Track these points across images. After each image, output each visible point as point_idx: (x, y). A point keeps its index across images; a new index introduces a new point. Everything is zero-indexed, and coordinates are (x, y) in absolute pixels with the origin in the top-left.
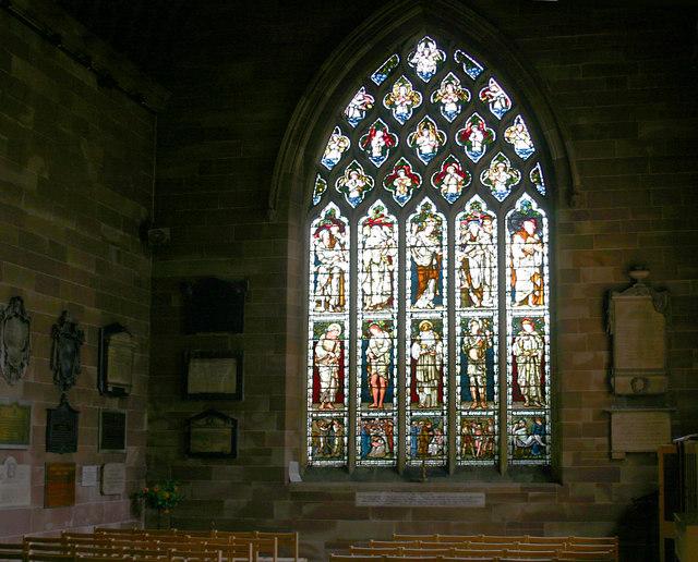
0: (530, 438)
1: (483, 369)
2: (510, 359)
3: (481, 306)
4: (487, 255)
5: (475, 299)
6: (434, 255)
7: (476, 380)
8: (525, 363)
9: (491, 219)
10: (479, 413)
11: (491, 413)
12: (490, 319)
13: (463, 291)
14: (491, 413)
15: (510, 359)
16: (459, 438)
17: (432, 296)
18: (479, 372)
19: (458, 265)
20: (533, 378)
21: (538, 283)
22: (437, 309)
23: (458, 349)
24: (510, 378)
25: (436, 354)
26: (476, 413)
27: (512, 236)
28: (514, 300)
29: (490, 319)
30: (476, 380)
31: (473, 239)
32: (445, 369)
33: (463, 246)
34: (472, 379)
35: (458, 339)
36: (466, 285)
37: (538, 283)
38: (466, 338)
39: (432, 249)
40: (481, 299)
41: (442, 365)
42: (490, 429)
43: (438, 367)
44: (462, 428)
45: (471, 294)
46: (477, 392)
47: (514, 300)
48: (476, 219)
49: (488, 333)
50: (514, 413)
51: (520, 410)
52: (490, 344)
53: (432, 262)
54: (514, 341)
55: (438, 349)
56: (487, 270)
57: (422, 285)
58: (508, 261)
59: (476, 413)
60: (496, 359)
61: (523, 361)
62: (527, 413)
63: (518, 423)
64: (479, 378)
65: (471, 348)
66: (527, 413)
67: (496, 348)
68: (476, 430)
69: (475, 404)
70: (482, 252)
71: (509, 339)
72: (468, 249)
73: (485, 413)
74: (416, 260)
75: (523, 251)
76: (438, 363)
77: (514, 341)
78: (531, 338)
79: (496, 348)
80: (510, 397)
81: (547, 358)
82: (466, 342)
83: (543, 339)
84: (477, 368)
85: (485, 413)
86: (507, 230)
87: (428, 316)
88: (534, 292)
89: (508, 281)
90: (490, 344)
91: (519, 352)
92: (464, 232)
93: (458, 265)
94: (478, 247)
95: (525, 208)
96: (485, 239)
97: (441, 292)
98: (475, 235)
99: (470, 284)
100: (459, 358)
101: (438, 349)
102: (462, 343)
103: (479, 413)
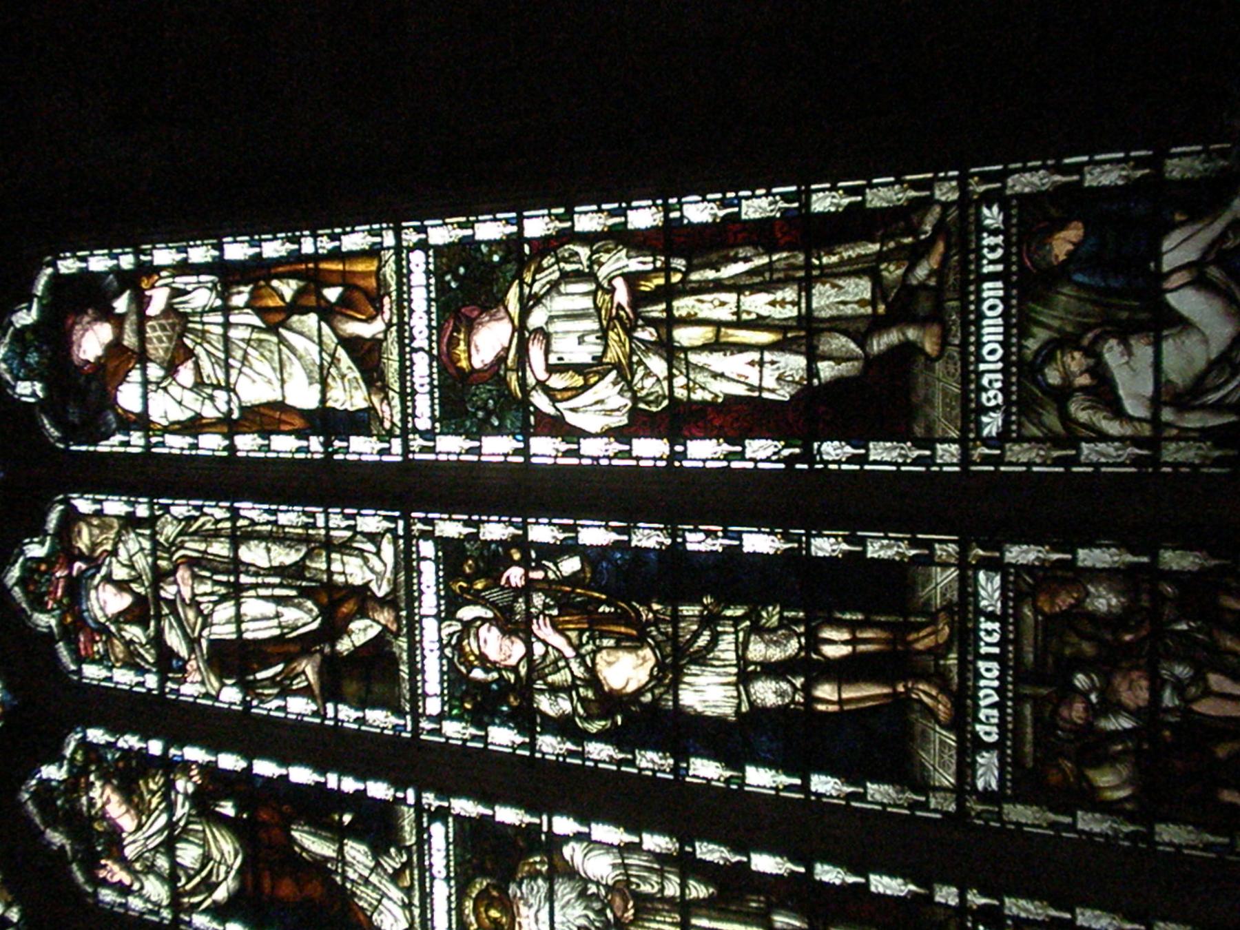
0: (1186, 301)
1: (709, 621)
2: (650, 449)
3: (389, 602)
4: (194, 547)
5: (362, 632)
6: (203, 803)
7: (772, 670)
8: (669, 350)
9: (71, 518)
10: (990, 672)
11: (989, 589)
12: (451, 552)
13: (330, 689)
14: (989, 589)
15: (650, 449)
16: (1168, 833)
17: (357, 852)
18: (726, 649)
19: (231, 695)
20: (757, 304)
21: (288, 288)
22: (411, 840)
23: (599, 751)
24: (761, 450)
25: (622, 888)
26: (987, 695)
27: (129, 423)
28: (361, 422)
29: (451, 552)
30: (772, 670)
31: (139, 612)
32: (710, 852)
33: (167, 662)
34: (767, 692)
35: (549, 745)
36: (309, 670)
37: (288, 288)
38: (544, 703)
39: (182, 810)
40: (362, 600)
41: (687, 866)
42: (1104, 601)
43: (698, 891)
44: (1093, 801)
45: (344, 646)
46: (841, 671)
47: (361, 422)
48: (77, 589)
49: (515, 575)
50: (992, 424)
51: (969, 378)
52: (570, 565)
53: (222, 821)
54: (556, 427)
55: (600, 867)
56: (252, 553)
57: (315, 889)
58: (211, 443)
59: (987, 695)
60: (649, 537)
61: (658, 365)
62: (992, 332)
63: (1062, 394)
64: (757, 650)
65: (593, 680)
66: (992, 332)
67: (594, 535)
68: (1110, 706)
69: (924, 692)
70: (183, 574)
71: (545, 448)
72: (174, 640)
73: (989, 634)
74: (221, 894)
75: (171, 369)
76: (672, 889)
77: (556, 427)
78: (537, 318)
79: (594, 535)
80: (882, 453)
81: (643, 217)
82: (565, 705)
83: (546, 246)
84: (701, 659)
85: (989, 634)
86: (103, 447)
87: (441, 892)
88: (327, 313)
89: (284, 445)
90: (570, 565)
91: (607, 390)
92: (119, 649)
93: (231, 695)
94: (168, 592)
95: (33, 358)
96: (134, 545)
97: (341, 800)
98: (125, 601)
99: (305, 644)
100: (649, 760)
101: (600, 867)
102: (563, 727)
103: (990, 672)
